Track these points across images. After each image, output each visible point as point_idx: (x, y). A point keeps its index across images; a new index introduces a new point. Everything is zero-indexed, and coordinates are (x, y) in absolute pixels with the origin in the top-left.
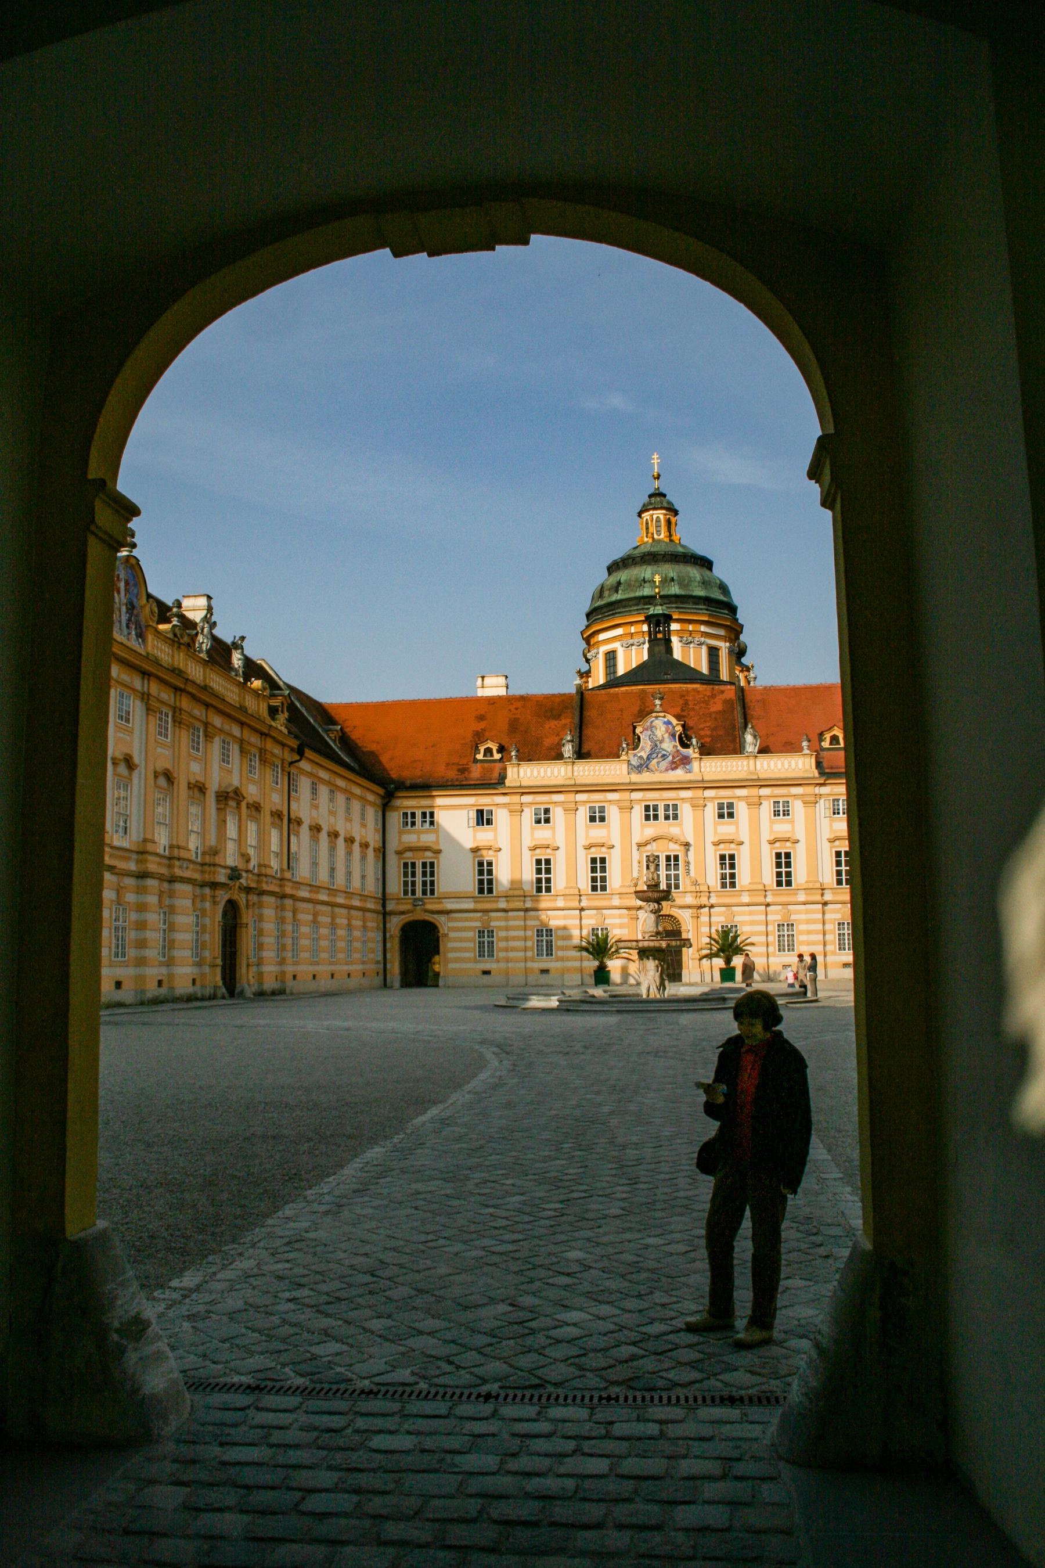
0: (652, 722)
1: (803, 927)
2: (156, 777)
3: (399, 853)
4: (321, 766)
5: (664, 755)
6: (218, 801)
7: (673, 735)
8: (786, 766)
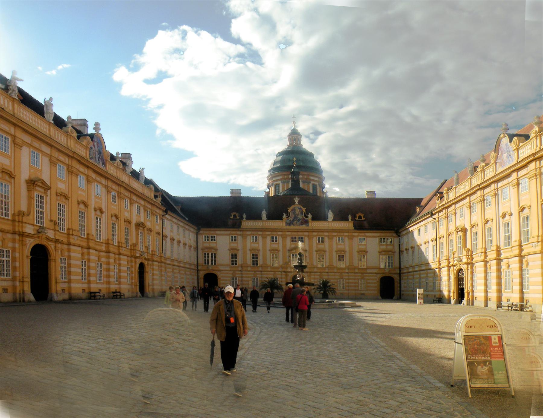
2: (112, 216)
3: (202, 249)
4: (174, 218)
5: (299, 220)
6: (136, 228)
7: (302, 213)
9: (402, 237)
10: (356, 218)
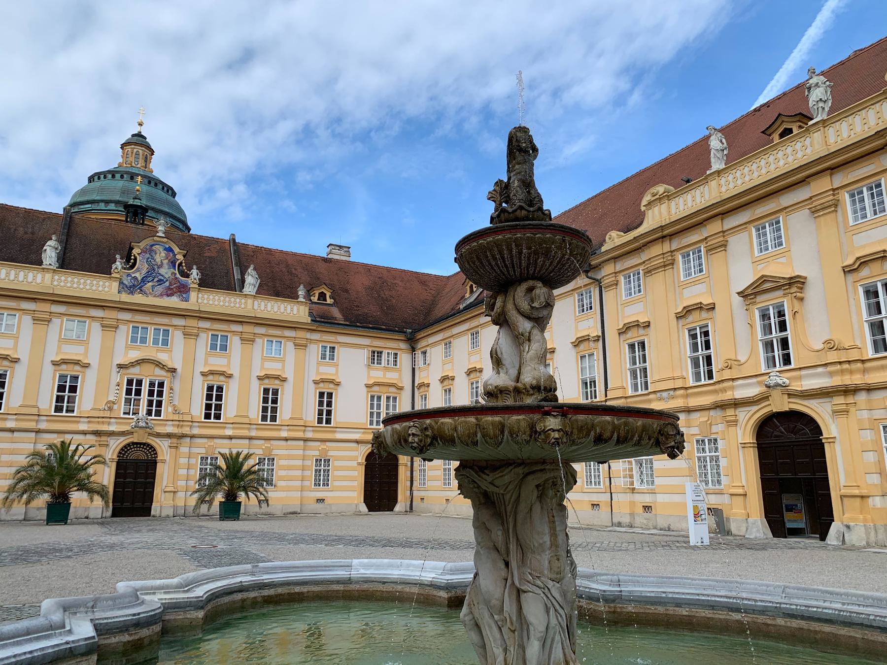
0: (152, 246)
1: (283, 462)
7: (173, 263)
8: (282, 310)
9: (424, 353)
10: (312, 298)
